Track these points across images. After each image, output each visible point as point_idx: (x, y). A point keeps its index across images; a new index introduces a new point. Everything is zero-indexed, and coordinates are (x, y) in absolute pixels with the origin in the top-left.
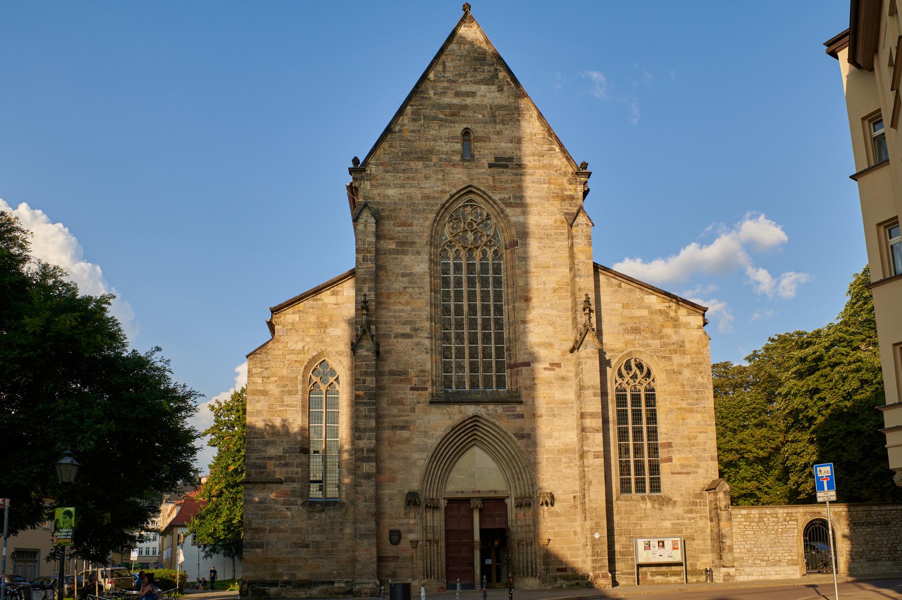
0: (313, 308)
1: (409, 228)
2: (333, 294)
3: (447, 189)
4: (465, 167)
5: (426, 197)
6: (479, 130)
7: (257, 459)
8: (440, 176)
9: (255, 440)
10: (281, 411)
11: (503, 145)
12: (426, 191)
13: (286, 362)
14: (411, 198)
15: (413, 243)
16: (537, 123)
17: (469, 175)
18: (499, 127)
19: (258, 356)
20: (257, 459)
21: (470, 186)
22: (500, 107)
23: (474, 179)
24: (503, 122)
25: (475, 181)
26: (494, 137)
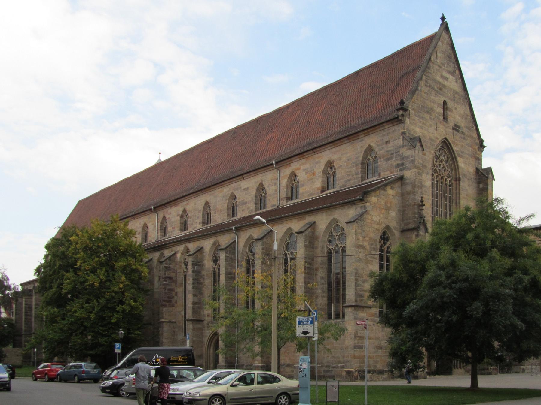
0: (383, 195)
1: (424, 156)
2: (392, 188)
3: (438, 137)
4: (444, 125)
5: (430, 139)
6: (450, 105)
7: (360, 291)
8: (436, 127)
9: (359, 278)
10: (370, 260)
11: (457, 117)
12: (431, 135)
13: (372, 229)
14: (424, 136)
15: (426, 166)
16: (468, 109)
17: (445, 131)
18: (456, 105)
19: (360, 221)
20: (360, 291)
21: (445, 138)
22: (456, 93)
23: (447, 134)
24: (458, 103)
25: (448, 136)
26: (454, 111)
